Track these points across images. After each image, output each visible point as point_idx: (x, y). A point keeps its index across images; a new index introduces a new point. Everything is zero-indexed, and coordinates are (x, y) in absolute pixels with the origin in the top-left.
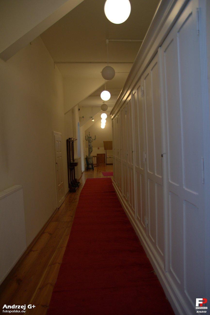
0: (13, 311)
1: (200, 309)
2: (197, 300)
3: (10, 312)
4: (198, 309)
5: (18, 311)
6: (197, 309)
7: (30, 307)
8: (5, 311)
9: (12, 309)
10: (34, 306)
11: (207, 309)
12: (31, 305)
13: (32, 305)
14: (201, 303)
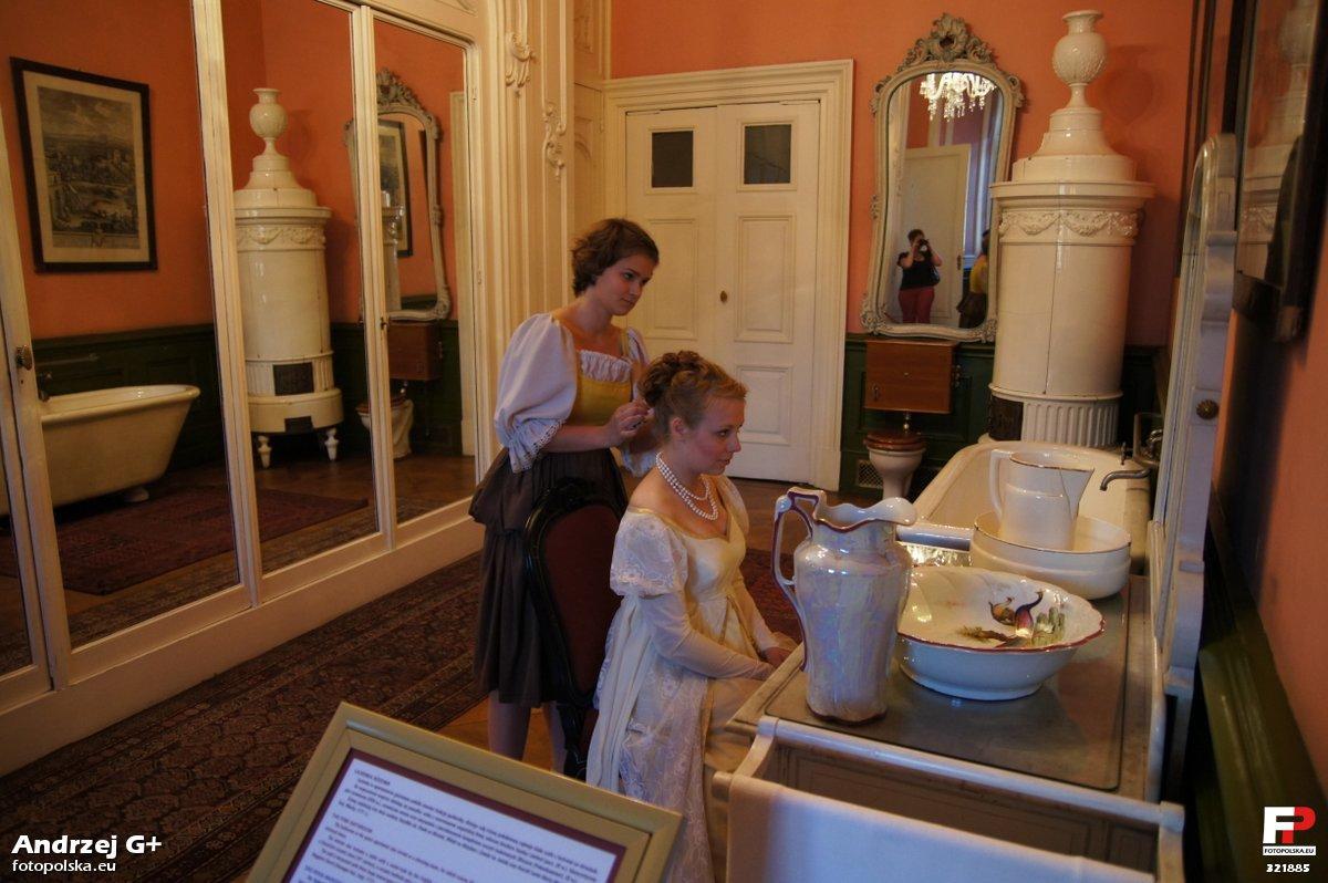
0: (59, 867)
3: (44, 868)
5: (82, 867)
7: (136, 844)
8: (23, 867)
9: (53, 858)
10: (154, 844)
12: (141, 838)
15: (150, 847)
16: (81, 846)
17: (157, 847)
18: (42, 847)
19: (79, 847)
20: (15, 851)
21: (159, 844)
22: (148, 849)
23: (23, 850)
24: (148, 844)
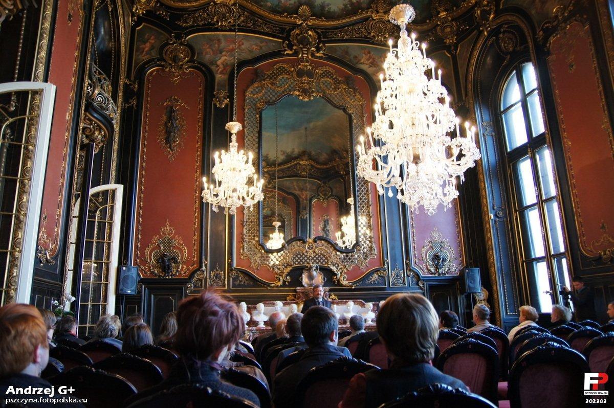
1: (594, 394)
2: (587, 376)
4: (588, 395)
6: (586, 395)
9: (25, 396)
10: (71, 390)
11: (608, 394)
12: (65, 387)
13: (68, 388)
14: (596, 382)
15: (70, 391)
16: (37, 391)
17: (72, 391)
18: (19, 391)
19: (36, 392)
20: (7, 393)
21: (74, 390)
22: (68, 392)
23: (10, 393)
24: (68, 390)
